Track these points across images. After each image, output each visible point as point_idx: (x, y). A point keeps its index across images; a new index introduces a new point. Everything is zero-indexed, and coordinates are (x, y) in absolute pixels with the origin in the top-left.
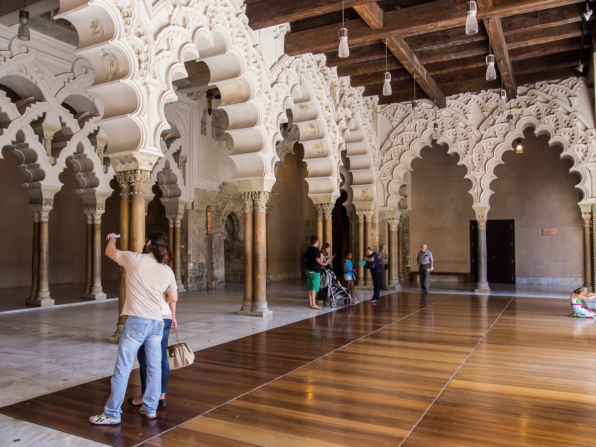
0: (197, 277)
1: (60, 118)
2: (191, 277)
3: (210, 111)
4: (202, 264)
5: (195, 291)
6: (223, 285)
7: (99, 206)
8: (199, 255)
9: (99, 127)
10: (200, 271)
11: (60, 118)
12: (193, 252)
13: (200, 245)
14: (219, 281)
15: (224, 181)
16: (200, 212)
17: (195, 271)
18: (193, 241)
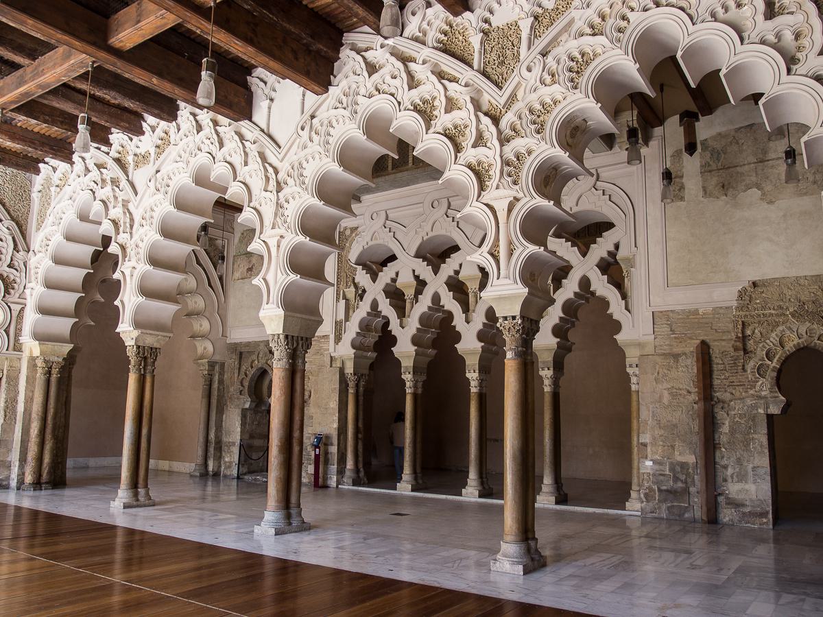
0: (667, 491)
1: (414, 271)
2: (650, 489)
3: (691, 148)
4: (684, 465)
5: (663, 519)
6: (767, 523)
7: (470, 367)
8: (673, 447)
9: (461, 265)
10: (676, 479)
11: (414, 271)
12: (654, 438)
13: (675, 426)
14: (747, 510)
15: (755, 279)
16: (676, 357)
17: (662, 478)
18: (653, 416)
